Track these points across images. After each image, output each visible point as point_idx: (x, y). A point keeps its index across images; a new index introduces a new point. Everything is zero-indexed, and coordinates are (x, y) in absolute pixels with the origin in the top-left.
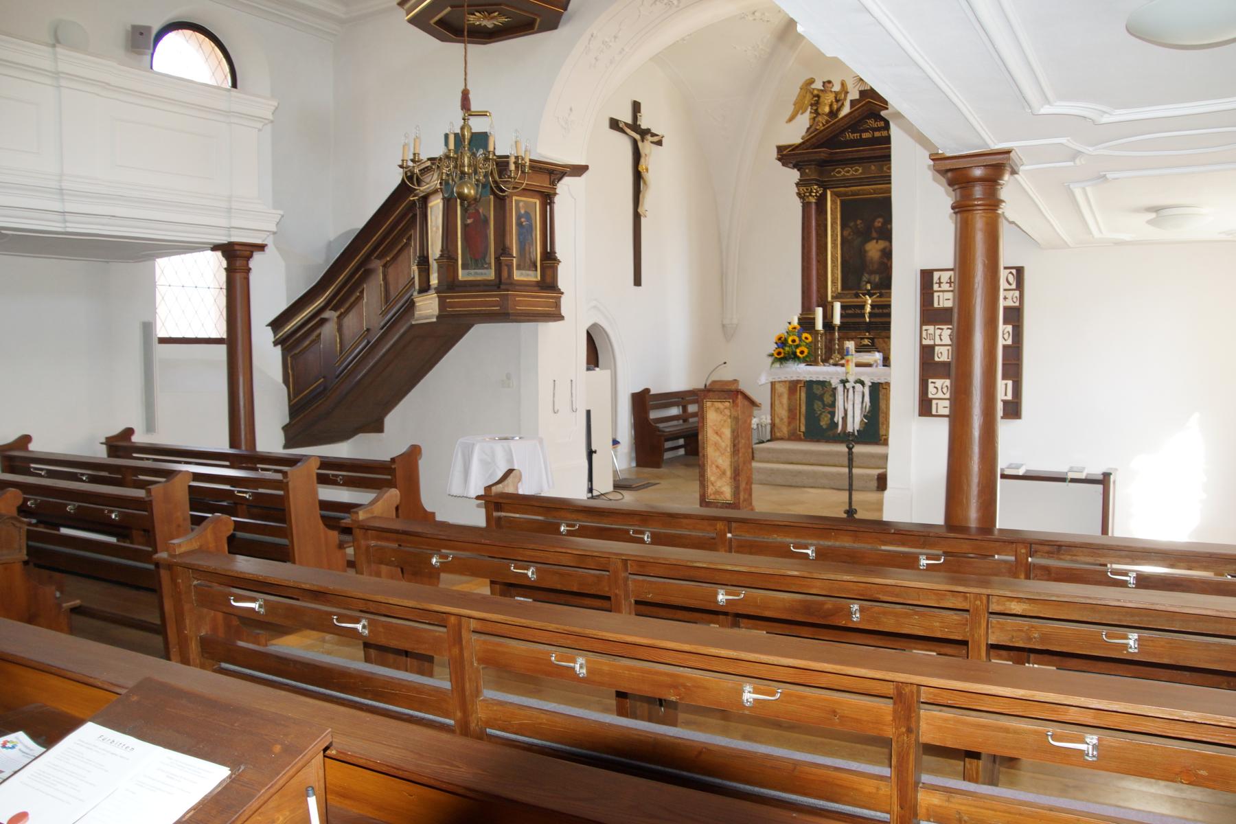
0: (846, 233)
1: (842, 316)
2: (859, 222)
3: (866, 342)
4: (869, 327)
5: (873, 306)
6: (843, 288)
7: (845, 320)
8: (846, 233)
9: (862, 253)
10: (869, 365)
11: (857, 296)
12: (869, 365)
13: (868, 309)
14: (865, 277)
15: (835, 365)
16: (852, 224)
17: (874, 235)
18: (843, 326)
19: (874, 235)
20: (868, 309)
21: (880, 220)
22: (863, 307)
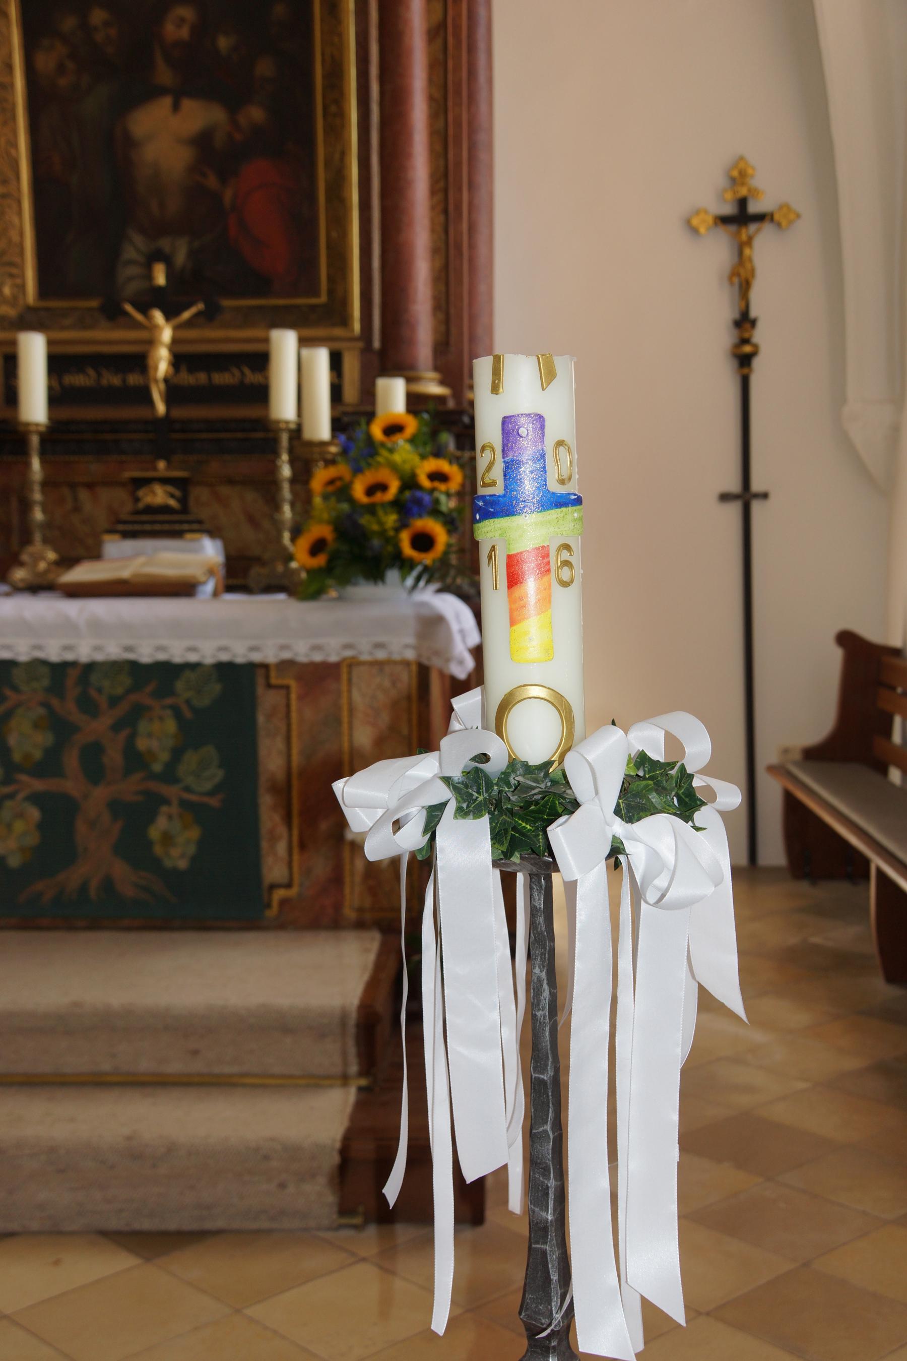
0: (45, 62)
1: (54, 399)
2: (98, 16)
3: (159, 496)
4: (164, 438)
5: (178, 360)
6: (45, 288)
7: (66, 413)
8: (45, 62)
9: (118, 150)
10: (184, 589)
11: (113, 313)
12: (184, 589)
13: (162, 362)
14: (134, 247)
15: (35, 588)
16: (69, 23)
17: (164, 75)
18: (57, 436)
19: (164, 75)
20: (162, 362)
21: (186, 12)
22: (140, 361)
